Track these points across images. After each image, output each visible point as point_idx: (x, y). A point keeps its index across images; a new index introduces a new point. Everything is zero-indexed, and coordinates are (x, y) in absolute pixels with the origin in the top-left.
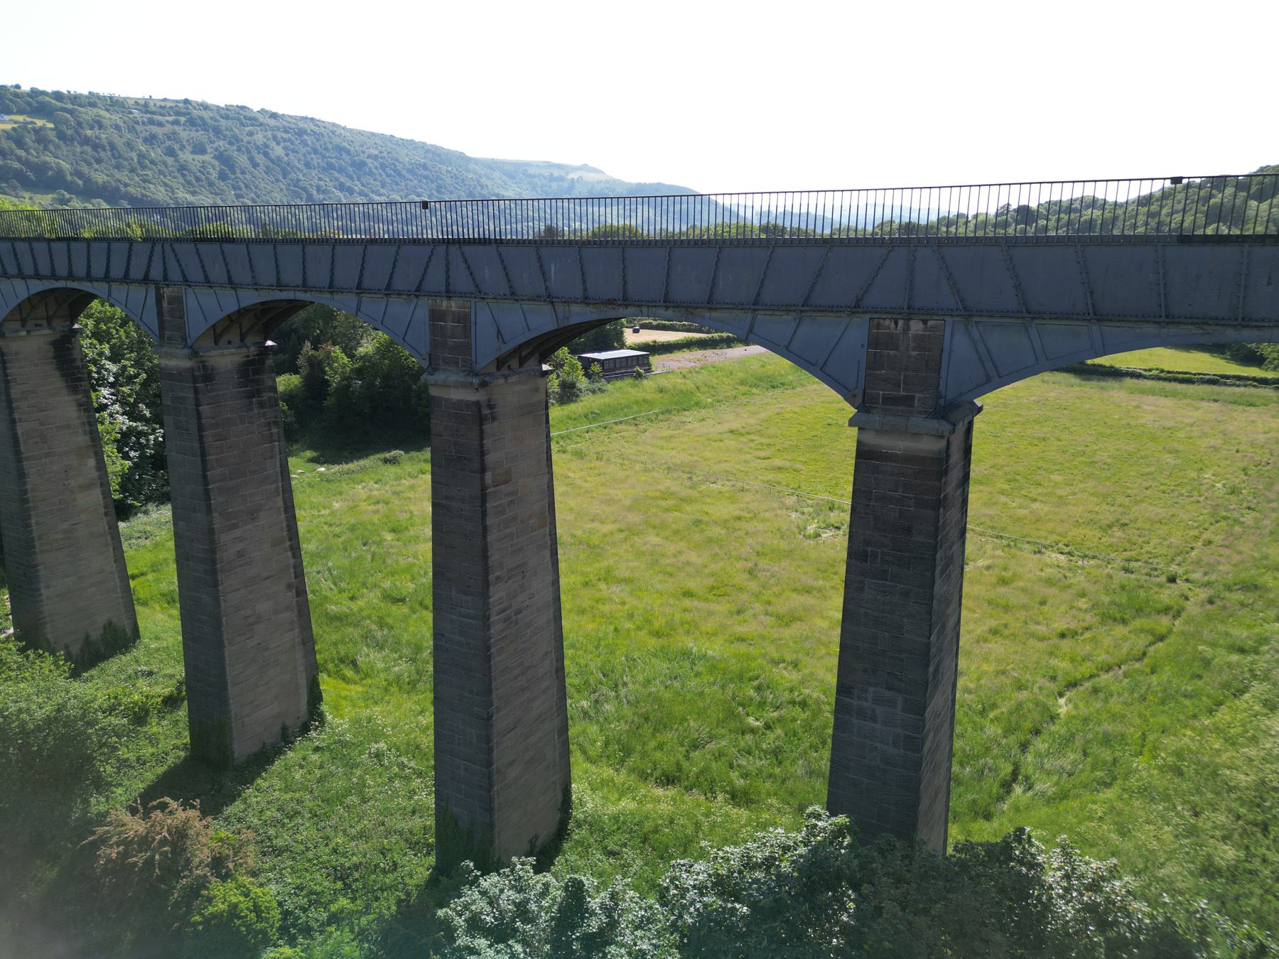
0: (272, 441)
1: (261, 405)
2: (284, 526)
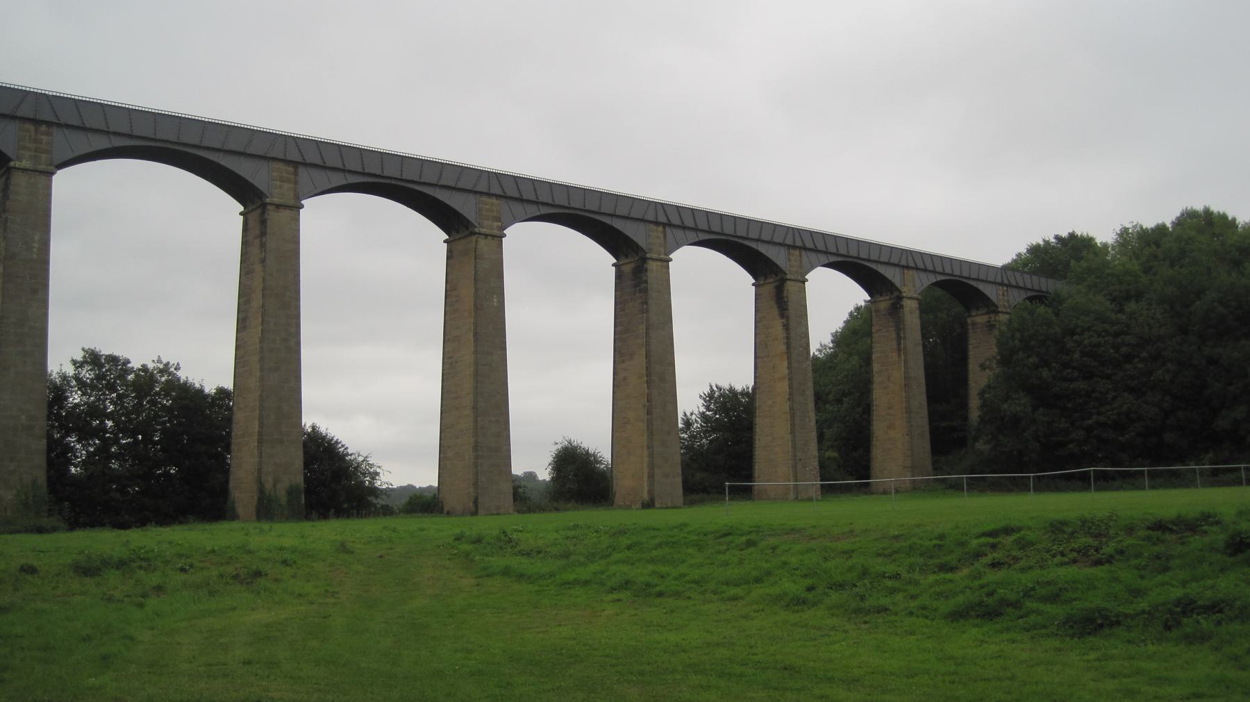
0: (643, 313)
1: (640, 291)
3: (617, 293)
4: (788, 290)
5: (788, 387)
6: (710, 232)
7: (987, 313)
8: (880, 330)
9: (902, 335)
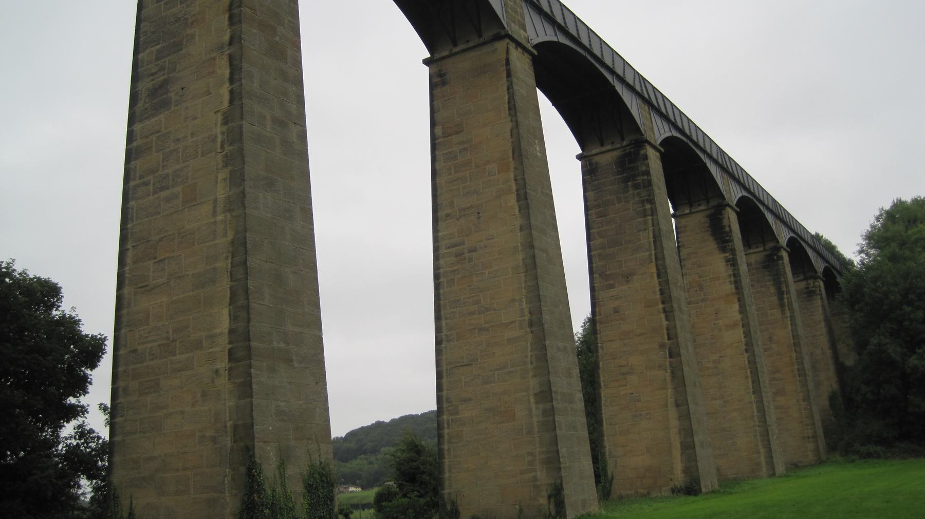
0: (645, 215)
1: (636, 187)
2: (657, 289)
3: (591, 194)
4: (729, 218)
5: (742, 335)
7: (806, 279)
9: (784, 289)
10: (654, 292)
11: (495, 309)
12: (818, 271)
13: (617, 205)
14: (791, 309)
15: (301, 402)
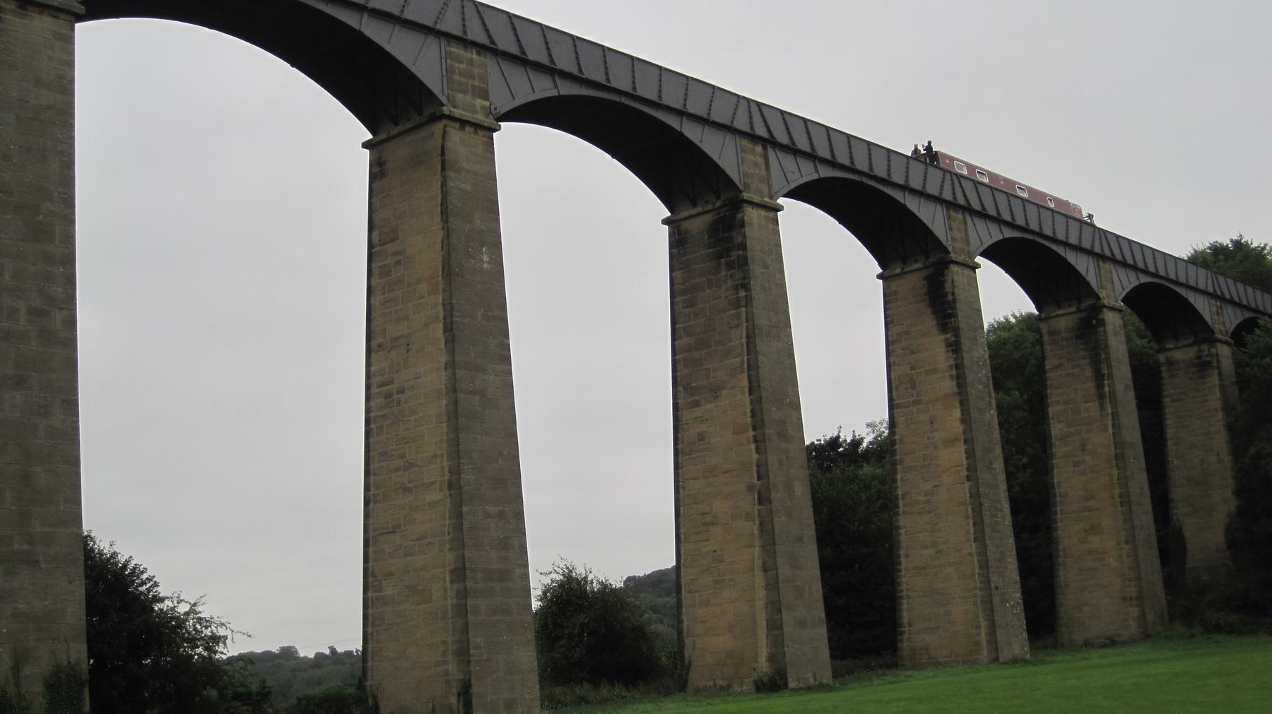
0: (738, 307)
1: (730, 266)
2: (749, 410)
3: (678, 273)
4: (953, 282)
5: (964, 456)
6: (833, 164)
8: (1061, 365)
9: (1105, 371)
10: (745, 414)
11: (418, 466)
12: (1217, 327)
13: (707, 291)
14: (1114, 403)
15: (47, 603)
